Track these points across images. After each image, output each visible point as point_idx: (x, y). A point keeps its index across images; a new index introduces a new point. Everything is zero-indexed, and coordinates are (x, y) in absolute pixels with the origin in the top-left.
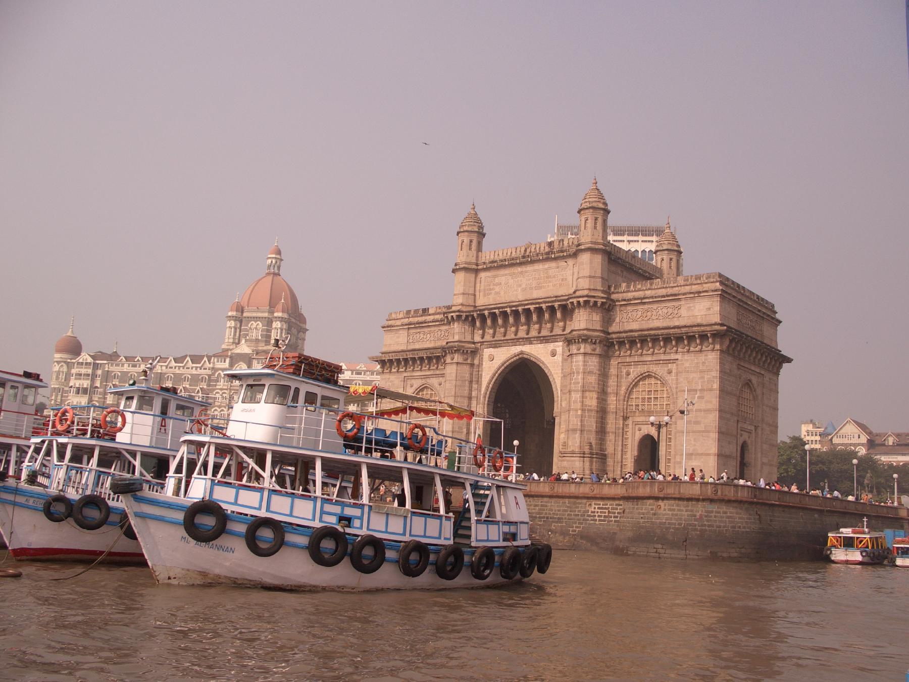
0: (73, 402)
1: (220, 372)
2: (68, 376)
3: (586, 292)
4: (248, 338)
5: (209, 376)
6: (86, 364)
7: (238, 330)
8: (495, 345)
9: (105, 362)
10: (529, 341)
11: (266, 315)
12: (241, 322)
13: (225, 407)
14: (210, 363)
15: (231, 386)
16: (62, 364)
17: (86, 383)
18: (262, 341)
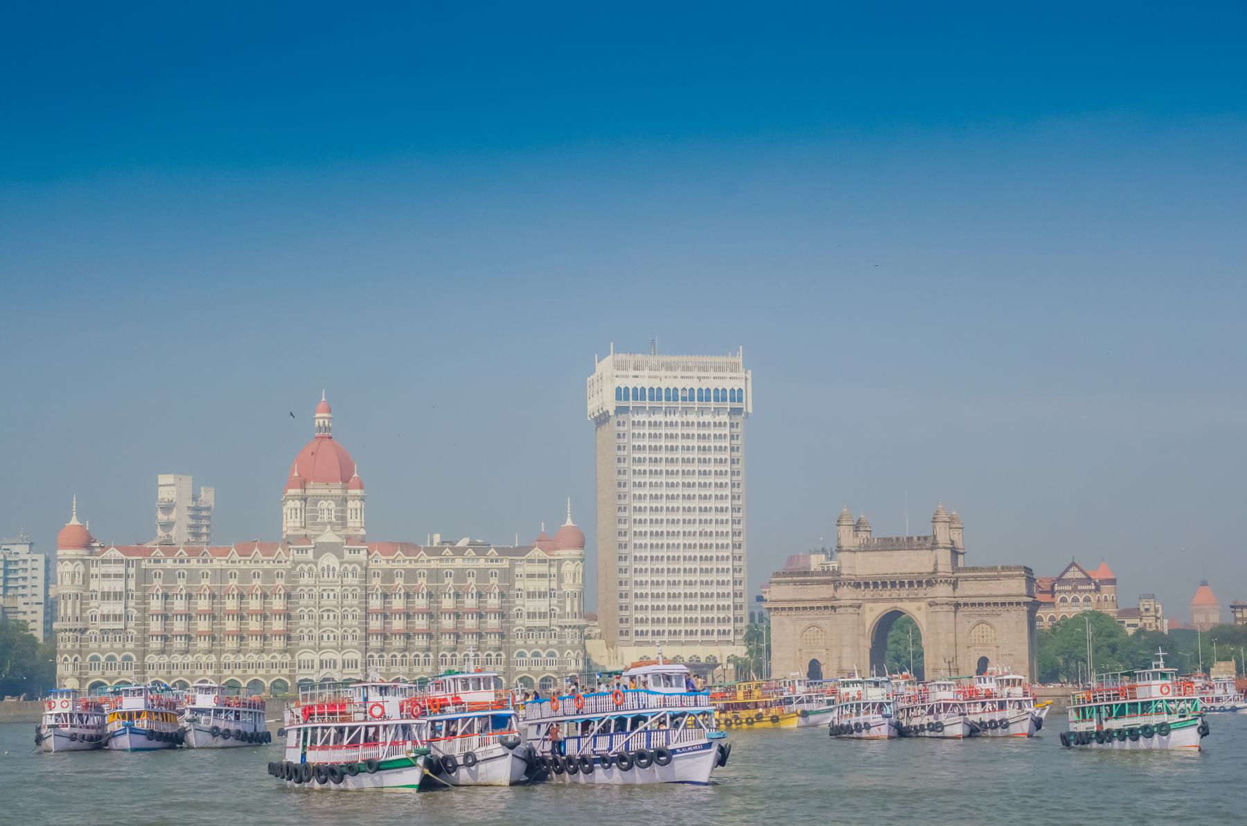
0: (102, 611)
1: (302, 565)
2: (86, 578)
3: (944, 574)
4: (318, 520)
5: (289, 571)
6: (116, 561)
7: (303, 511)
8: (875, 601)
9: (141, 558)
10: (901, 600)
11: (339, 492)
12: (305, 500)
13: (315, 608)
14: (288, 555)
15: (319, 582)
16: (78, 562)
17: (119, 586)
18: (338, 524)
